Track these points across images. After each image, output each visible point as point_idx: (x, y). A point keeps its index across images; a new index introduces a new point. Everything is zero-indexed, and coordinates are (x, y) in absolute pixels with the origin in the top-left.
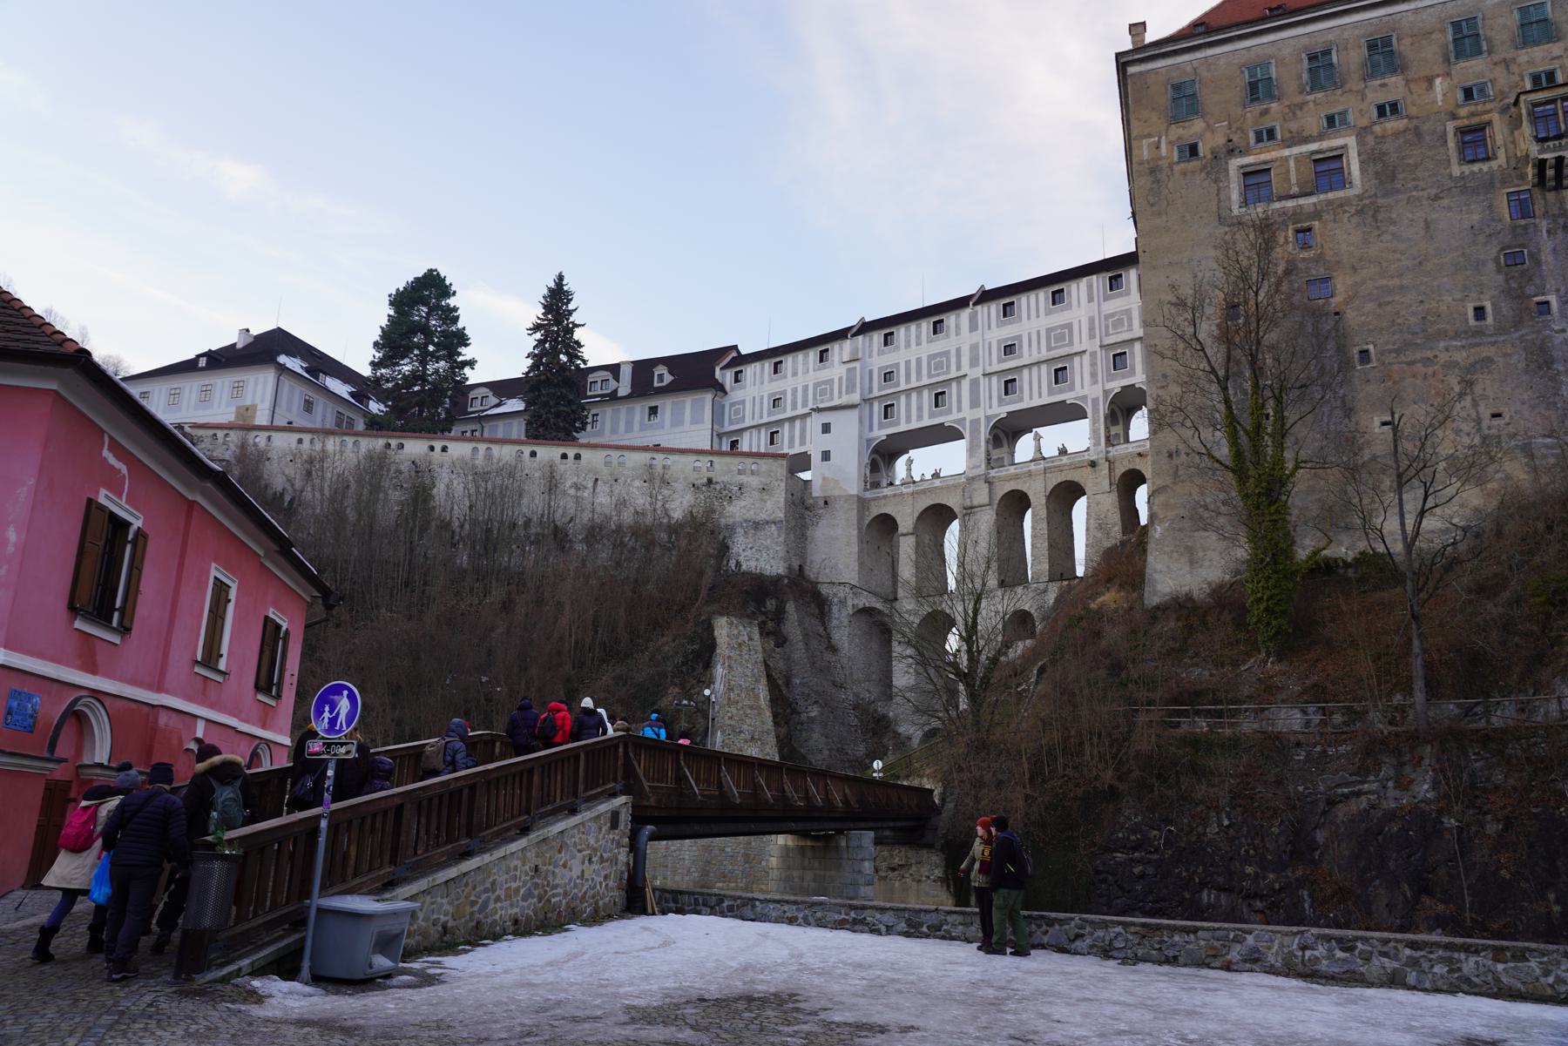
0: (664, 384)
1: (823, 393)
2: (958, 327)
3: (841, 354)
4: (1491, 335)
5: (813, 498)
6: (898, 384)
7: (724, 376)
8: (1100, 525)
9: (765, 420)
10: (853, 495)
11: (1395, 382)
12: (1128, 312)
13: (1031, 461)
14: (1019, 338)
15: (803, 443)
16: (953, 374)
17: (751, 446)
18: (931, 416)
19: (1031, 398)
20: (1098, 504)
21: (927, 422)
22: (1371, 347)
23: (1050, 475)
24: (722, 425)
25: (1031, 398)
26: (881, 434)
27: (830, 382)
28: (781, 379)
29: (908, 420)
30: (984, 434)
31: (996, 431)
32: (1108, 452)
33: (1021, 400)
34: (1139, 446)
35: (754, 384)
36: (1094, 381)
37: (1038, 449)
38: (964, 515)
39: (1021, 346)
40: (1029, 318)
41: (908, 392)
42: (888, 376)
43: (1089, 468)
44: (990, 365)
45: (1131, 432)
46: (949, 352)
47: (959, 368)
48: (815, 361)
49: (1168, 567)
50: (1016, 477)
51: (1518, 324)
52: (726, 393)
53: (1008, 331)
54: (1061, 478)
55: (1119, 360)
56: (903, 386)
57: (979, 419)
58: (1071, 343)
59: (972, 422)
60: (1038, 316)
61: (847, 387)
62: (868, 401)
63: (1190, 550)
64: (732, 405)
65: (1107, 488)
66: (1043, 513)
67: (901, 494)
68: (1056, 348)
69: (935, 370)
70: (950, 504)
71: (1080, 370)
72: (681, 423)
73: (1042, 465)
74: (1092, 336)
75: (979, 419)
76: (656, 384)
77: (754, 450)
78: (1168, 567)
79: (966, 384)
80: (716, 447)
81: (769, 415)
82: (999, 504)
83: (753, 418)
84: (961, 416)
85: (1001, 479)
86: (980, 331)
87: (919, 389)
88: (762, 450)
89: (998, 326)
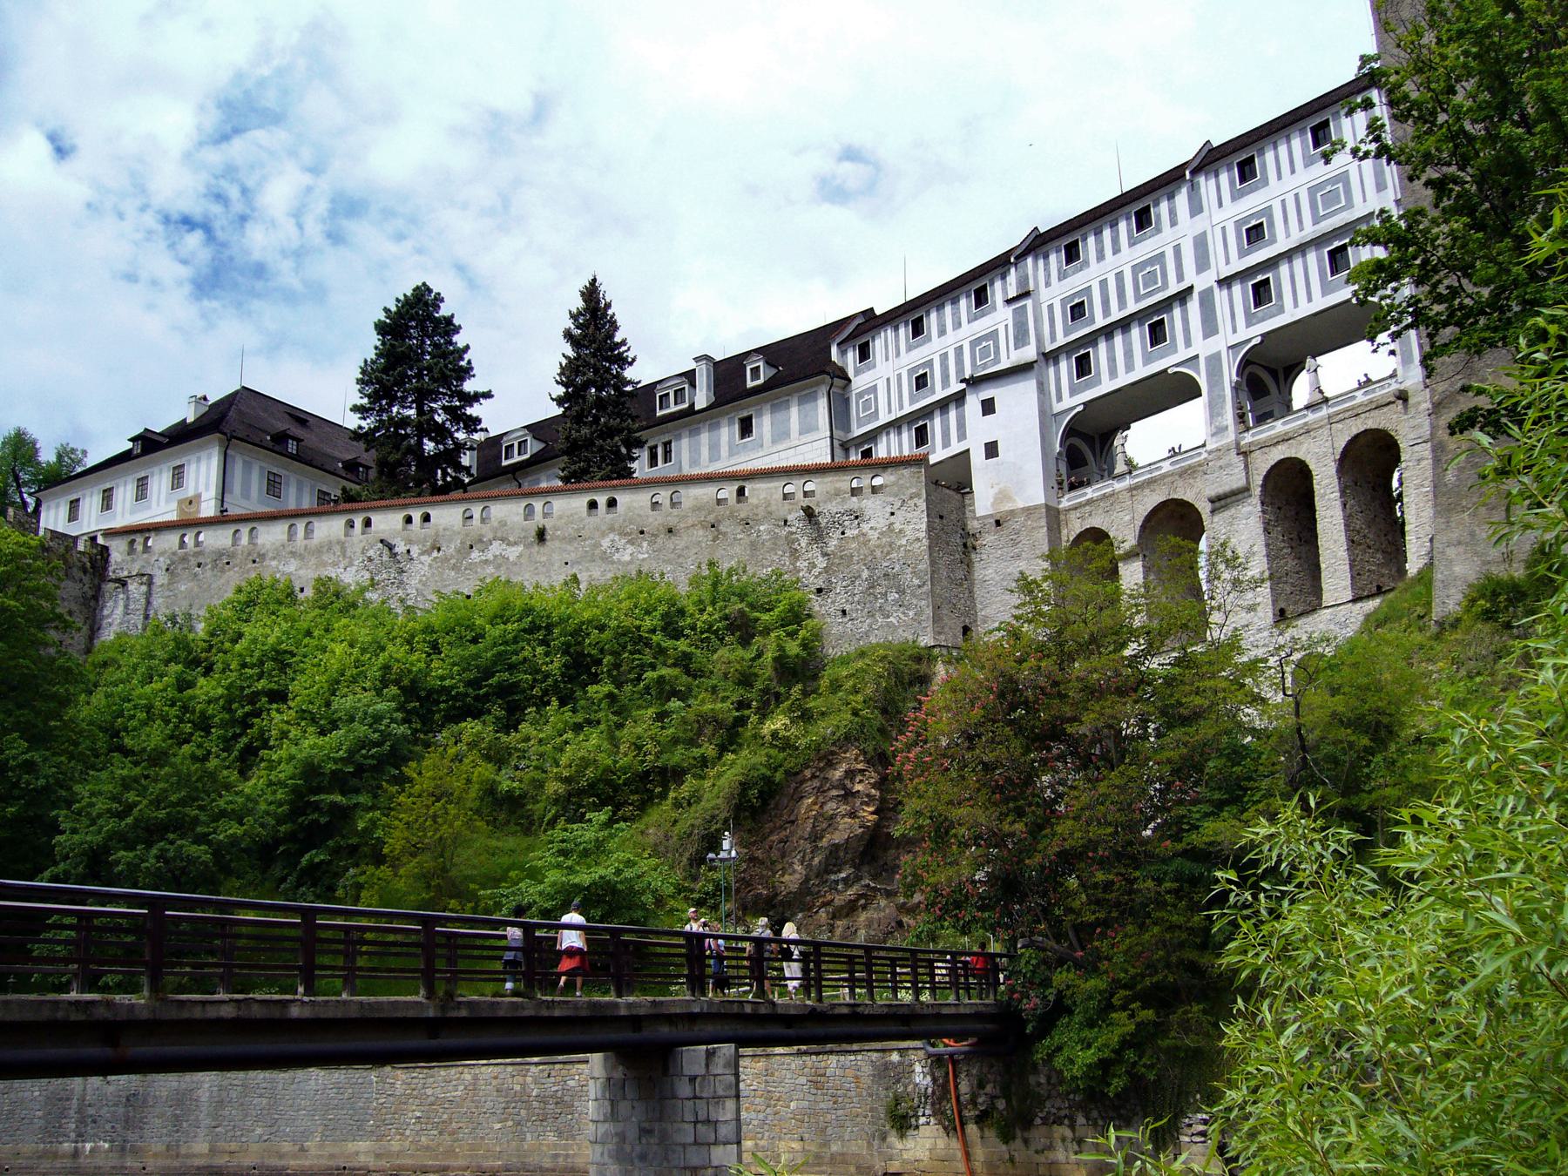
0: (761, 381)
1: (985, 353)
2: (1173, 213)
3: (1005, 290)
5: (978, 519)
6: (1093, 321)
7: (843, 353)
9: (908, 409)
10: (1036, 507)
14: (1268, 212)
15: (962, 436)
16: (1174, 288)
17: (889, 451)
18: (1147, 360)
19: (1296, 305)
21: (1141, 371)
23: (1340, 426)
24: (848, 429)
25: (1296, 305)
26: (1071, 401)
27: (993, 335)
28: (924, 343)
29: (1113, 373)
30: (1229, 374)
31: (1249, 369)
33: (1281, 310)
35: (887, 359)
39: (1271, 224)
40: (1280, 177)
41: (1108, 332)
42: (1078, 311)
44: (1228, 262)
46: (1162, 254)
47: (1180, 278)
48: (969, 307)
50: (1285, 439)
52: (850, 381)
53: (1252, 203)
54: (1356, 427)
56: (1100, 322)
57: (1219, 353)
58: (1350, 204)
59: (1209, 359)
60: (1293, 172)
61: (1016, 338)
62: (1051, 357)
64: (860, 395)
68: (1325, 217)
69: (1145, 286)
72: (786, 434)
75: (1219, 353)
76: (750, 384)
77: (895, 453)
79: (1194, 305)
80: (839, 459)
81: (912, 401)
82: (1264, 486)
83: (890, 411)
84: (1190, 353)
85: (1264, 446)
86: (1206, 213)
87: (1124, 325)
88: (906, 453)
89: (1234, 199)
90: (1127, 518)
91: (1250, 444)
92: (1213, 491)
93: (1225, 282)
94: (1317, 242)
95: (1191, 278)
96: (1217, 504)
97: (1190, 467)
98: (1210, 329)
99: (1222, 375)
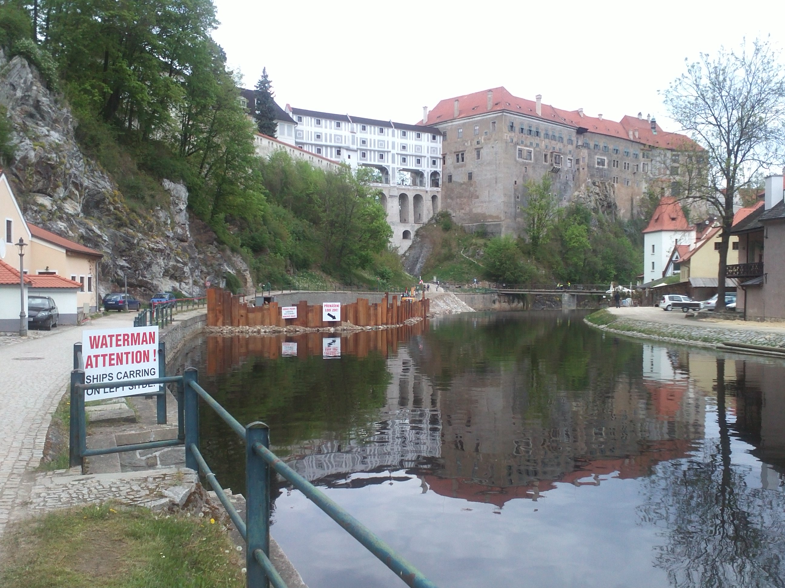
12: (437, 148)
36: (428, 167)
50: (404, 189)
55: (434, 163)
71: (424, 161)
74: (428, 152)
79: (390, 155)
93: (398, 154)
94: (416, 156)
95: (390, 149)
98: (393, 162)
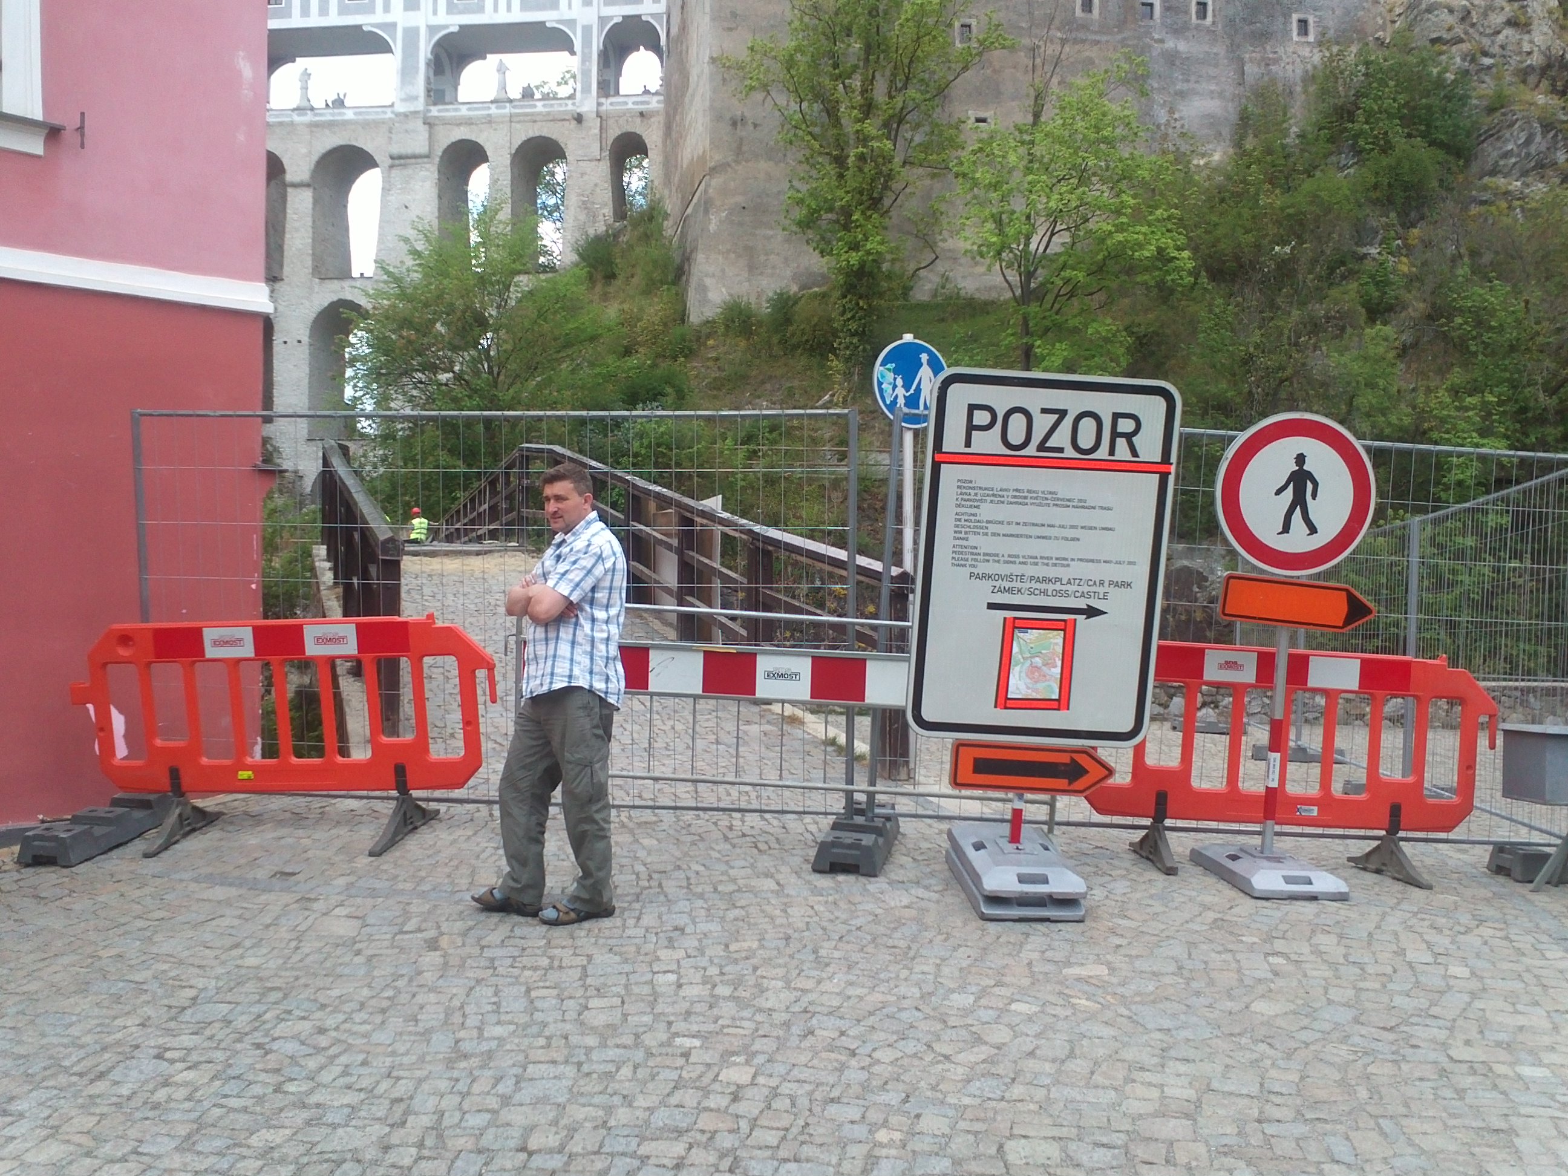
4: (1095, 33)
8: (584, 202)
11: (995, 71)
13: (492, 102)
20: (582, 175)
22: (973, 22)
23: (518, 126)
30: (424, 51)
32: (599, 104)
34: (642, 103)
37: (503, 87)
38: (391, 167)
43: (574, 123)
45: (622, 80)
49: (723, 271)
50: (469, 122)
51: (1121, 25)
54: (534, 131)
63: (750, 252)
65: (597, 154)
66: (506, 180)
67: (292, 124)
70: (369, 147)
73: (508, 110)
78: (723, 271)
82: (442, 157)
90: (304, 151)
91: (437, 117)
92: (396, 150)
96: (397, 162)
97: (374, 121)
99: (417, 49)
